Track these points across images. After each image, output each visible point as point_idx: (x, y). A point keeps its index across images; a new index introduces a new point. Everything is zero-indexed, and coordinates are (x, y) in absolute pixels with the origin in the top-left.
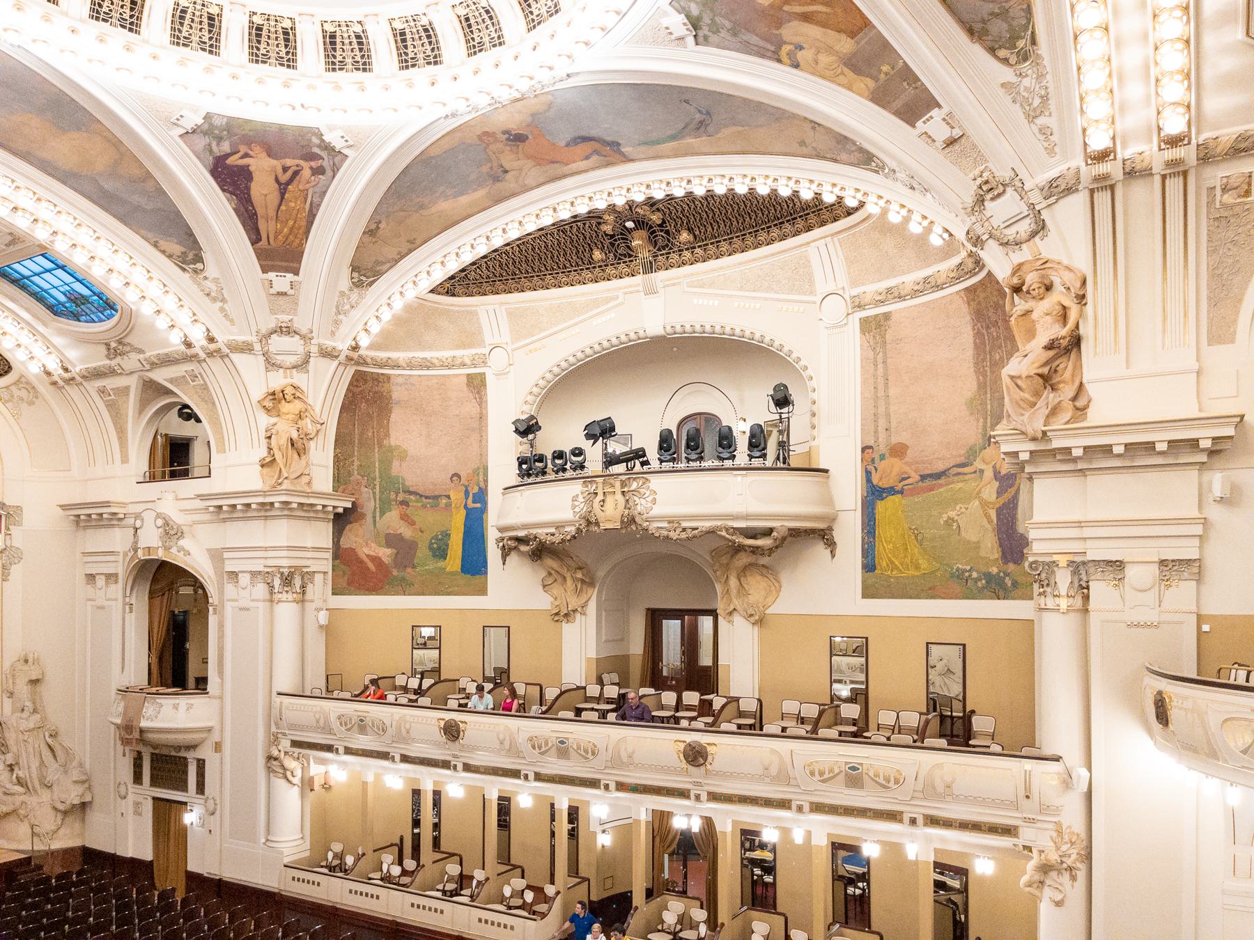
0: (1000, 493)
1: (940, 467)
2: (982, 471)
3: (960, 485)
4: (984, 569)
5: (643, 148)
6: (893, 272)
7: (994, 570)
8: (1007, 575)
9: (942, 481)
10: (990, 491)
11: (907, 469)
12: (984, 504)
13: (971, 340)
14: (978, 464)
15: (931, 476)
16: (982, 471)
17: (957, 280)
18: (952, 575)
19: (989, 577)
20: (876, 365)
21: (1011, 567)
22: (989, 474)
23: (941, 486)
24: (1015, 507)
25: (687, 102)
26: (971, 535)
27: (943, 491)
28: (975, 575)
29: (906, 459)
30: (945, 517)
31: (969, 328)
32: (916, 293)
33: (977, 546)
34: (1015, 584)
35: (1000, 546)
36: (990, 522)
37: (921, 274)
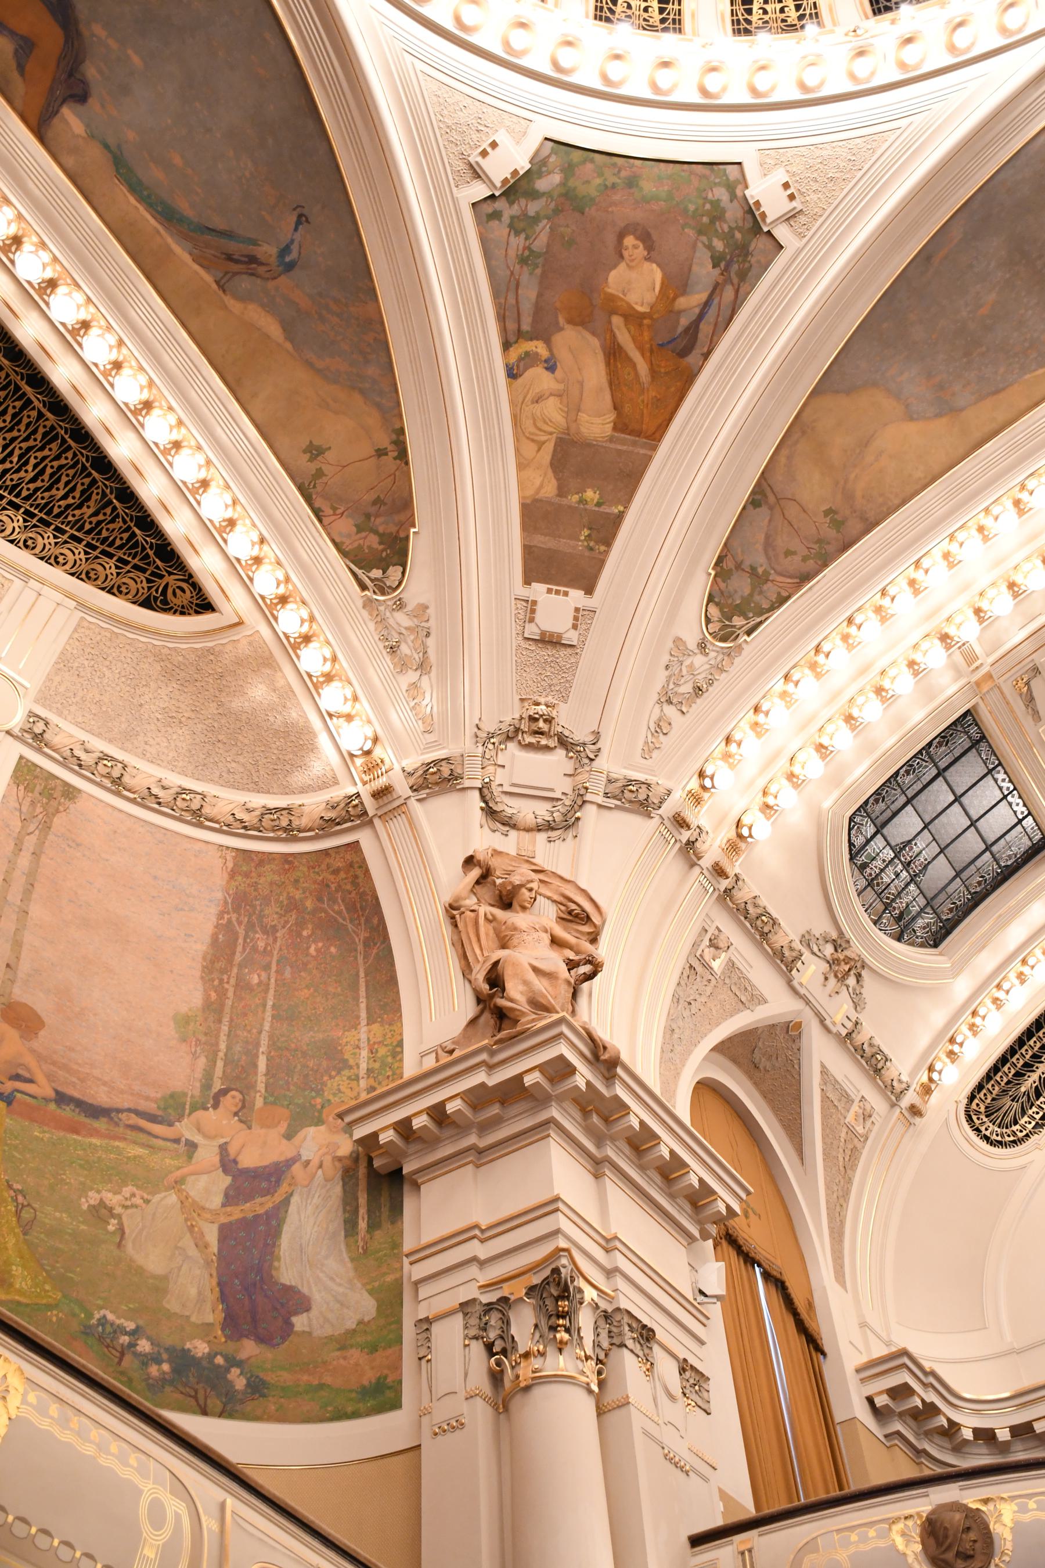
0: (231, 1198)
1: (102, 1097)
2: (192, 1146)
3: (140, 1151)
4: (169, 1340)
5: (95, 153)
6: (125, 739)
7: (200, 1348)
8: (232, 1362)
9: (101, 1124)
10: (209, 1187)
11: (30, 1061)
12: (191, 1209)
13: (209, 928)
14: (185, 1129)
15: (79, 1104)
16: (192, 1146)
17: (245, 829)
18: (87, 1331)
19: (183, 1361)
20: (18, 848)
21: (249, 1349)
22: (208, 1154)
23: (96, 1133)
24: (274, 1233)
25: (302, 219)
26: (153, 1260)
27: (95, 1142)
28: (144, 1346)
29: (35, 1044)
30: (93, 1198)
31: (214, 910)
32: (148, 799)
33: (160, 1286)
34: (257, 1388)
35: (223, 1298)
36: (202, 1245)
37: (176, 780)
